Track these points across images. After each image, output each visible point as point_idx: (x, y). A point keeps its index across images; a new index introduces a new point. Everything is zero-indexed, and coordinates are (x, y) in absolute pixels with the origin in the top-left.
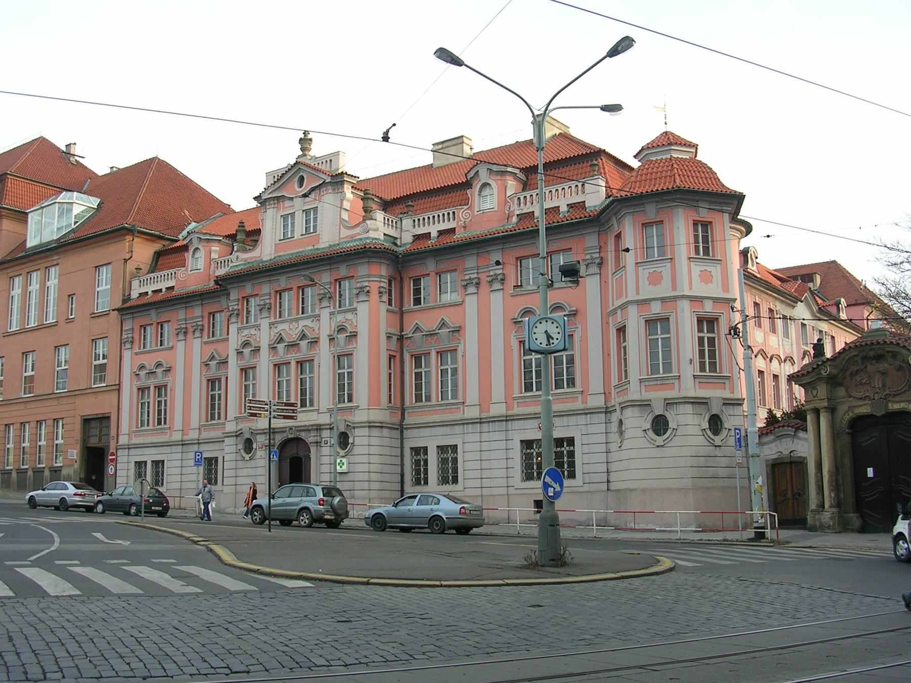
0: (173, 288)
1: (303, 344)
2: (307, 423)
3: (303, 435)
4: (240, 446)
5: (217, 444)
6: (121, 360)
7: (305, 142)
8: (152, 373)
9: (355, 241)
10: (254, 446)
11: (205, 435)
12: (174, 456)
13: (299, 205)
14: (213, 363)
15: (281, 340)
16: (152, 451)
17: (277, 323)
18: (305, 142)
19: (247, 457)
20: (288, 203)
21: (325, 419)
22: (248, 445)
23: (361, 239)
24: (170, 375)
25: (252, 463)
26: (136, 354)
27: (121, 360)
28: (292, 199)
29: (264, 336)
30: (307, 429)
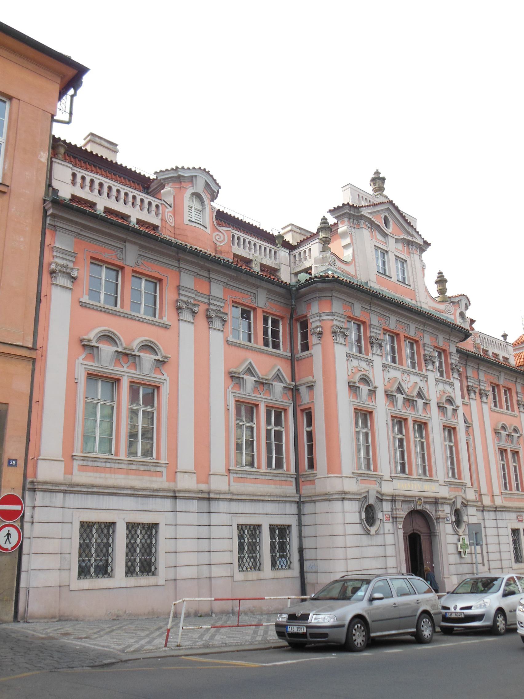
0: (155, 228)
1: (420, 402)
2: (437, 495)
3: (429, 508)
4: (363, 515)
5: (248, 504)
6: (39, 301)
7: (378, 181)
8: (126, 356)
9: (443, 316)
10: (380, 516)
11: (239, 487)
12: (182, 518)
13: (392, 246)
14: (250, 380)
15: (400, 390)
16: (129, 503)
17: (390, 366)
18: (378, 181)
19: (373, 530)
20: (379, 237)
21: (444, 492)
22: (370, 516)
23: (447, 318)
24: (165, 369)
25: (379, 540)
26: (84, 305)
27: (39, 301)
28: (385, 235)
29: (379, 379)
30: (436, 502)
